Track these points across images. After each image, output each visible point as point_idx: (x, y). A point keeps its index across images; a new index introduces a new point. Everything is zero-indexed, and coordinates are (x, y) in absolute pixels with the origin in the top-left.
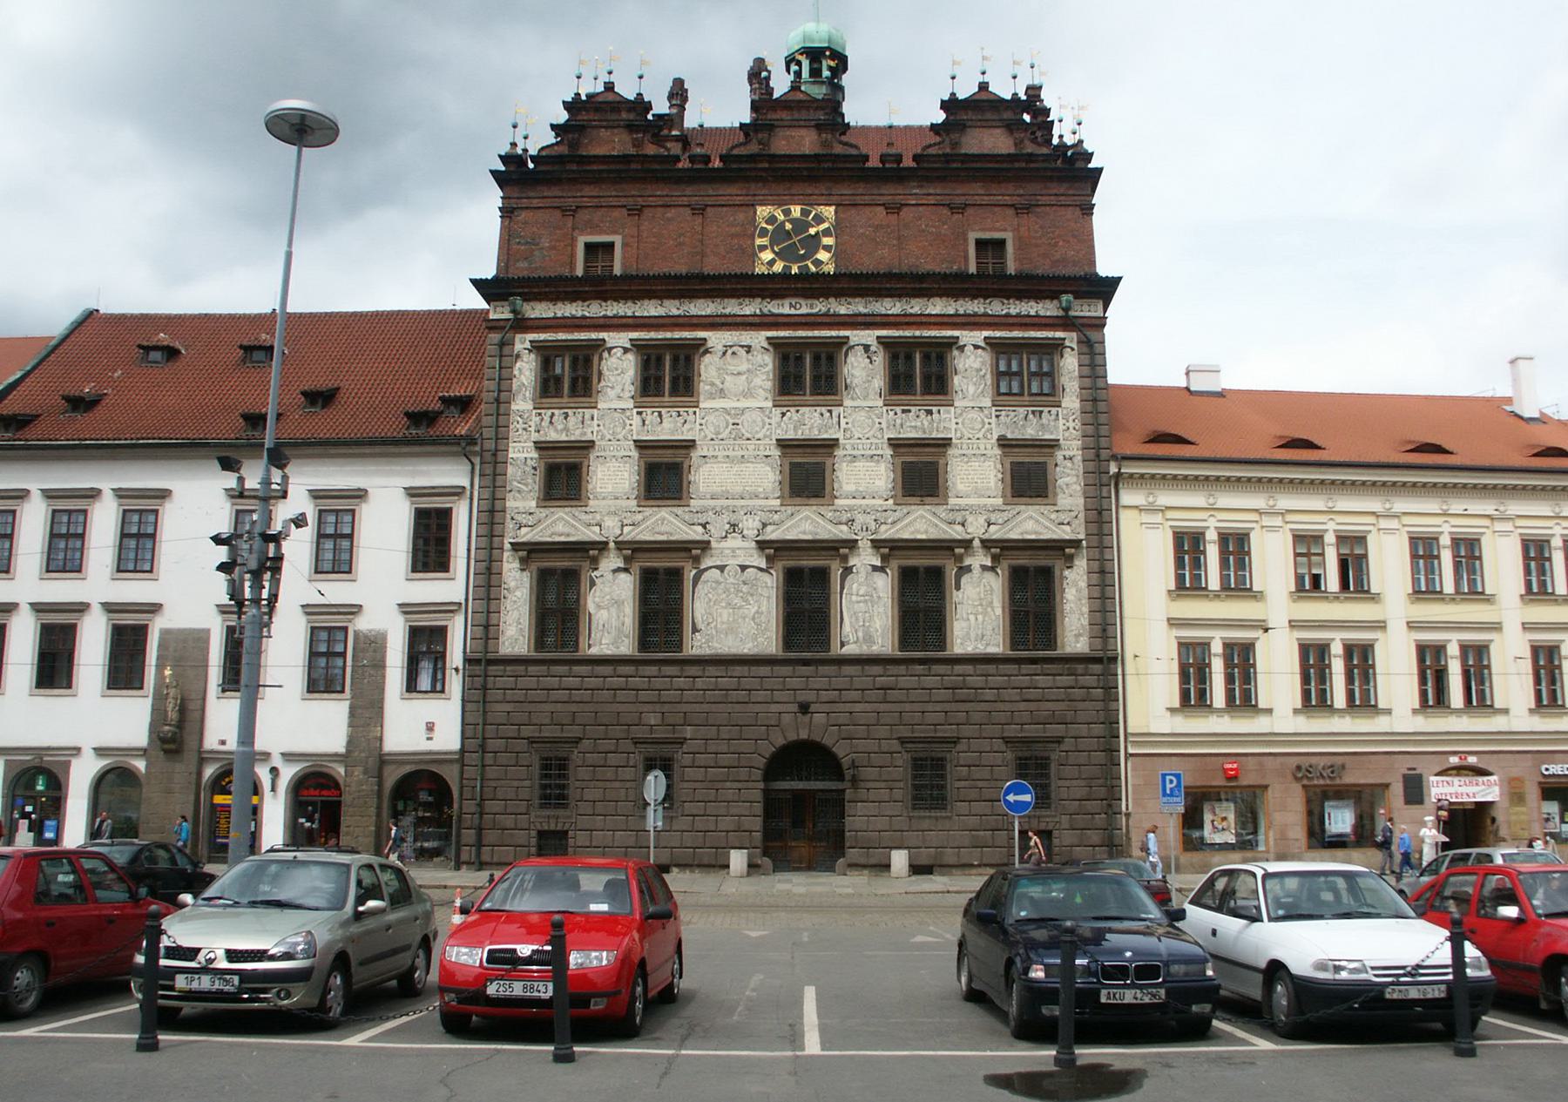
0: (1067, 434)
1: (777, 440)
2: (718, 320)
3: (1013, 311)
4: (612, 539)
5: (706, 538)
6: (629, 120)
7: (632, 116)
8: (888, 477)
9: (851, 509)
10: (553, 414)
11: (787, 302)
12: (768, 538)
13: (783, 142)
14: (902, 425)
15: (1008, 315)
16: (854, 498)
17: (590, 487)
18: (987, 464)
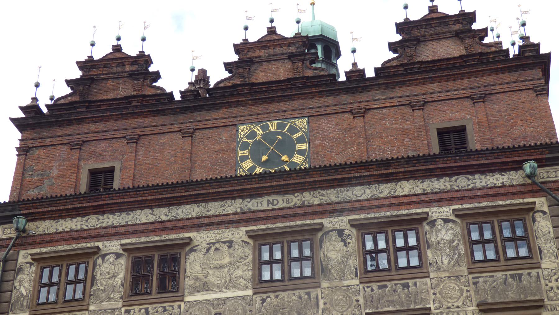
0: (552, 294)
2: (202, 221)
3: (478, 185)
6: (131, 71)
7: (134, 68)
11: (265, 200)
13: (262, 74)
15: (473, 189)
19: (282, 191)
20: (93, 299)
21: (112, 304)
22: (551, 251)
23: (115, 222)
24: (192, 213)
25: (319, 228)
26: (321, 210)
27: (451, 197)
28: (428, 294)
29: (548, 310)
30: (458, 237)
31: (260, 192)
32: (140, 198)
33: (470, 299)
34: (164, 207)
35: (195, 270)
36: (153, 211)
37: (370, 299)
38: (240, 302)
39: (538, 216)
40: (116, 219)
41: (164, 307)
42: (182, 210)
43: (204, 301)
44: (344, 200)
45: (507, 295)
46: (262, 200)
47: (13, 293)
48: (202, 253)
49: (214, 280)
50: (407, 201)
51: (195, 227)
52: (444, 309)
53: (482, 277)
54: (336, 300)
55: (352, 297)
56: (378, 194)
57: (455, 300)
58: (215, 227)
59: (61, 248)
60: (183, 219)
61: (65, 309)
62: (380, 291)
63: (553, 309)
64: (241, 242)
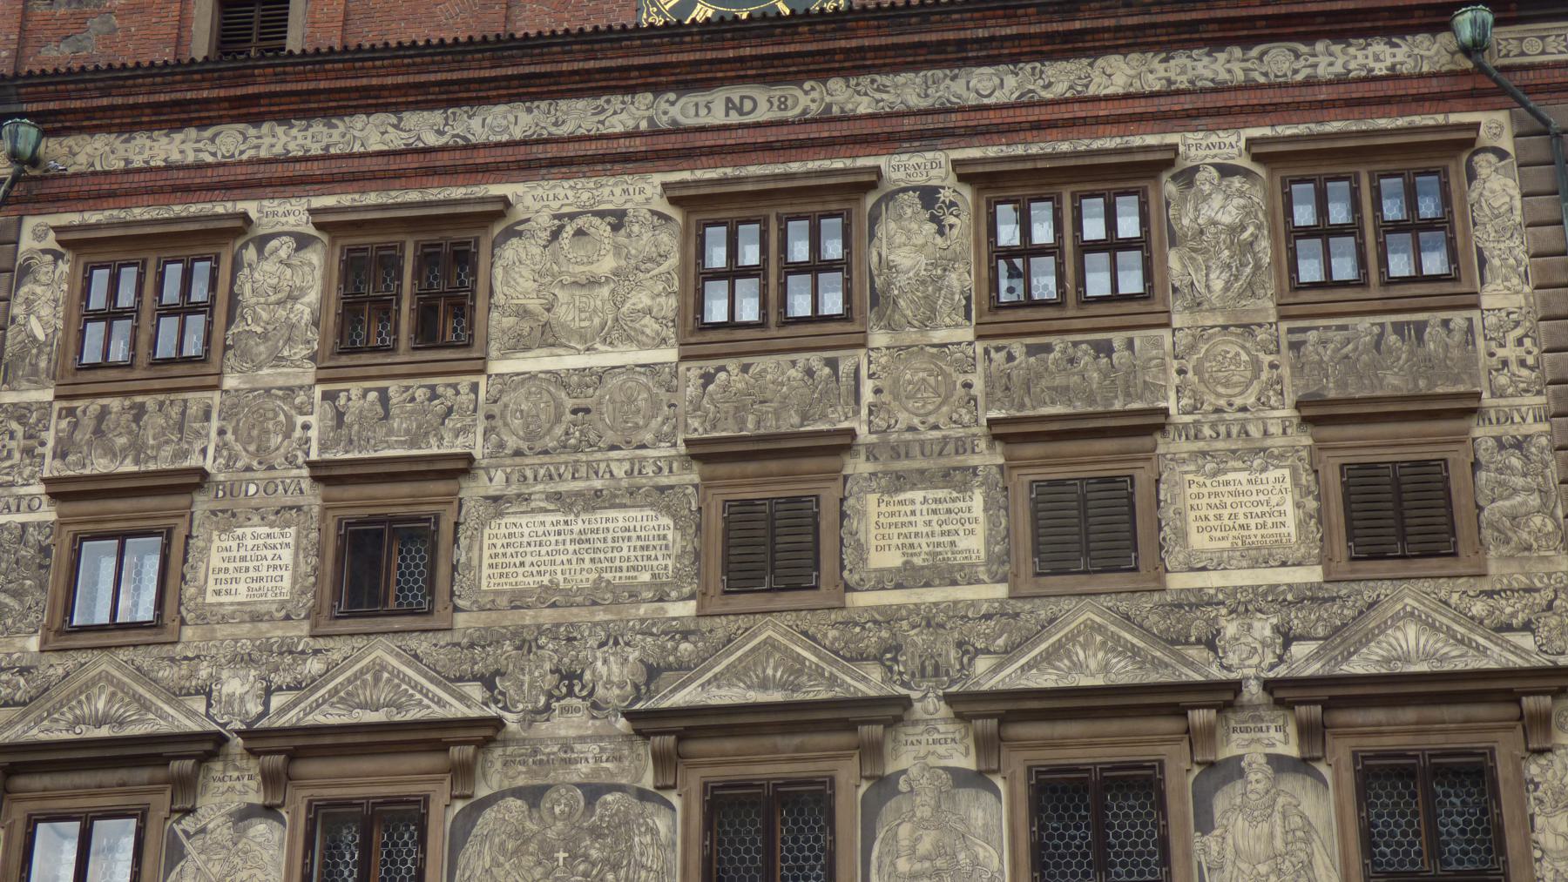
0: (1503, 380)
1: (689, 443)
2: (538, 152)
3: (1323, 72)
4: (238, 725)
5: (493, 711)
8: (992, 523)
9: (888, 617)
10: (104, 412)
11: (718, 97)
12: (666, 704)
14: (1027, 386)
15: (1309, 83)
16: (899, 586)
17: (190, 591)
18: (1272, 474)
19: (767, 75)
20: (232, 360)
21: (288, 374)
22: (1512, 261)
23: (292, 146)
24: (511, 127)
25: (870, 182)
26: (878, 130)
27: (1244, 103)
28: (1165, 371)
29: (1491, 422)
30: (1256, 217)
31: (703, 76)
32: (365, 82)
33: (1279, 387)
34: (432, 109)
35: (518, 289)
36: (400, 120)
37: (1004, 381)
38: (643, 379)
39: (1484, 164)
40: (295, 138)
41: (433, 388)
42: (484, 120)
43: (543, 376)
44: (943, 103)
45: (1381, 380)
46: (709, 98)
47: (9, 334)
48: (540, 242)
49: (570, 318)
50: (1119, 112)
51: (520, 169)
52: (1206, 413)
53: (1317, 328)
54: (910, 382)
55: (954, 375)
56: (1038, 90)
57: (1238, 390)
58: (574, 169)
59: (138, 213)
60: (485, 146)
61: (157, 384)
62: (1032, 359)
63: (1503, 420)
64: (648, 215)
